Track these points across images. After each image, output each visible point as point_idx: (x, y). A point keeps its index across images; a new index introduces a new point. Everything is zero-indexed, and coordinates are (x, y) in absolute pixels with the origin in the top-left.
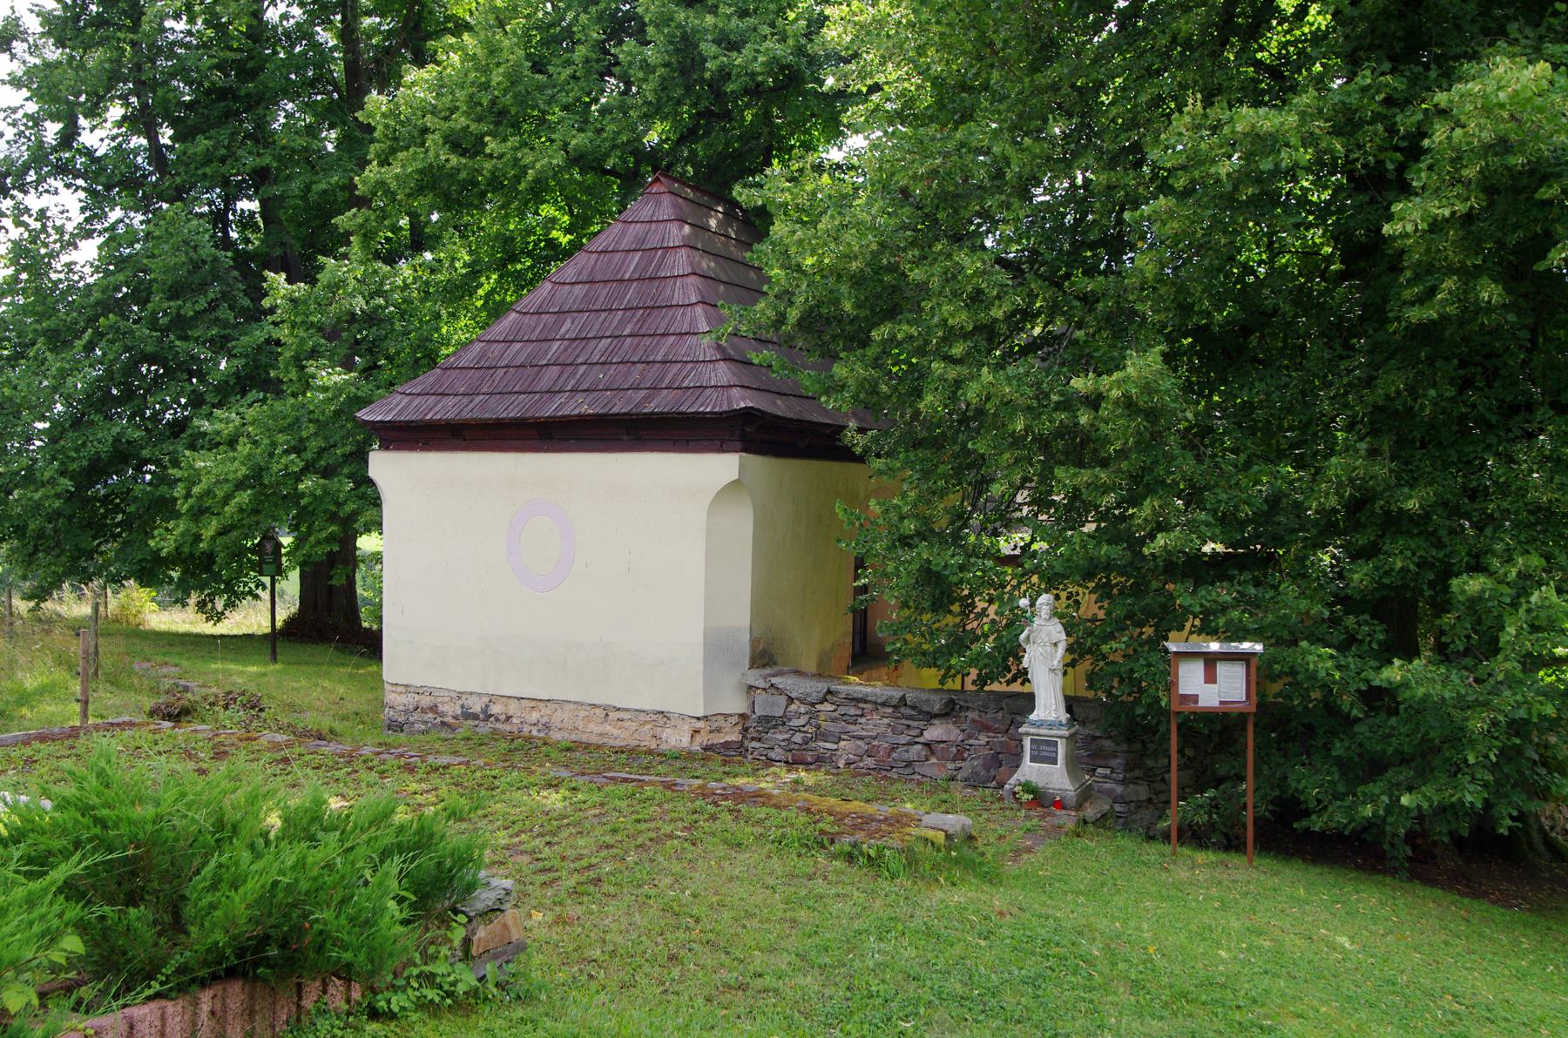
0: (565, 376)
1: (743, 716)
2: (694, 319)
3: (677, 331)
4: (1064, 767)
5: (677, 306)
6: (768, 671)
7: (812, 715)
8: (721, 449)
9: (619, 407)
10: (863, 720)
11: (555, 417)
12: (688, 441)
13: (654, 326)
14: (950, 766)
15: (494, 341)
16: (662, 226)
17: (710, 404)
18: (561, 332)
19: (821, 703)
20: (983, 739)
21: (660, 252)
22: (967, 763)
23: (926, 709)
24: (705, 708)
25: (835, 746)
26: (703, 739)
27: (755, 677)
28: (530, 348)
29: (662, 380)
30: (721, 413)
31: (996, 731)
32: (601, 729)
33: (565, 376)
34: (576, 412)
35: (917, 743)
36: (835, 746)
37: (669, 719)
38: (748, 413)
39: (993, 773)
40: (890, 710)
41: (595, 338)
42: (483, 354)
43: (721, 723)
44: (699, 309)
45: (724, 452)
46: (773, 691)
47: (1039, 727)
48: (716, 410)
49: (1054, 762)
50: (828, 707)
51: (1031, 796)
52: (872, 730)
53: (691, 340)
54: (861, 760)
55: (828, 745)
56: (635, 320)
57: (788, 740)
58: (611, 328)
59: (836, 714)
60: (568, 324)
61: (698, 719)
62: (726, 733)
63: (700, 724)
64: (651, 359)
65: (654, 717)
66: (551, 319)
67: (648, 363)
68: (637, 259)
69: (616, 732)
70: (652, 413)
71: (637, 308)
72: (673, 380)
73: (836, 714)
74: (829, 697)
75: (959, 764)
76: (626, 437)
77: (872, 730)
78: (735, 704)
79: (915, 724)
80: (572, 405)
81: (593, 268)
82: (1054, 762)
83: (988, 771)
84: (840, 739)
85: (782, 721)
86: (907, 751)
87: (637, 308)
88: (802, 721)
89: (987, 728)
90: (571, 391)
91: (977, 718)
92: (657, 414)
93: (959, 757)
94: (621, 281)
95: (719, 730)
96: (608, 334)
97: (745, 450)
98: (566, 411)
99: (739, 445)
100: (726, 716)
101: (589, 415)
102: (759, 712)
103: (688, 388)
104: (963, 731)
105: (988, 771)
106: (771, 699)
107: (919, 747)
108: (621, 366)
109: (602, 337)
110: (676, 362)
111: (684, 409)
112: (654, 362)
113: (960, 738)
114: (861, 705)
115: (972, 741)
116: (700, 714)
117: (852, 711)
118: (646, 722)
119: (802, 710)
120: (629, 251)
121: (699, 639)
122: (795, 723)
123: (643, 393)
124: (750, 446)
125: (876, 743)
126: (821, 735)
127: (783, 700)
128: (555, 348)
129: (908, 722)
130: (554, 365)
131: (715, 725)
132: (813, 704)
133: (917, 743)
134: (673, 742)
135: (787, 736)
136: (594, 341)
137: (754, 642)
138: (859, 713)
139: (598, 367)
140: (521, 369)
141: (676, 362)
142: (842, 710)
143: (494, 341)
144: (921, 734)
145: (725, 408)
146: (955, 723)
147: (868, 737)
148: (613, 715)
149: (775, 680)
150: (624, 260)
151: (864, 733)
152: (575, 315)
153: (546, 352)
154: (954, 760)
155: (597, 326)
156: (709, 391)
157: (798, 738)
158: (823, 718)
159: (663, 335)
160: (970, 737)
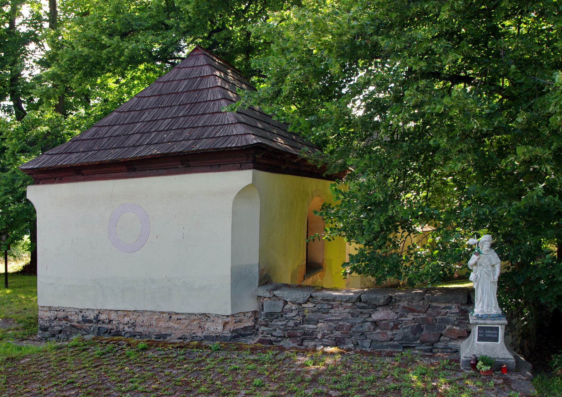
0: (144, 138)
1: (255, 312)
2: (220, 105)
3: (211, 112)
4: (503, 343)
5: (210, 101)
6: (270, 287)
7: (301, 310)
8: (241, 168)
9: (177, 148)
10: (332, 311)
11: (136, 157)
12: (219, 165)
13: (196, 111)
14: (389, 333)
15: (103, 126)
16: (199, 68)
17: (234, 143)
18: (142, 118)
19: (306, 303)
20: (410, 317)
21: (199, 79)
22: (401, 330)
23: (374, 302)
24: (232, 310)
25: (315, 327)
26: (231, 327)
27: (263, 292)
28: (124, 127)
29: (203, 134)
30: (242, 147)
31: (419, 312)
32: (167, 325)
33: (144, 138)
34: (150, 153)
35: (367, 321)
36: (315, 327)
37: (209, 317)
38: (257, 147)
39: (418, 336)
40: (350, 304)
41: (162, 119)
42: (96, 132)
43: (243, 317)
44: (223, 102)
45: (242, 169)
46: (275, 298)
47: (485, 319)
48: (239, 145)
49: (496, 340)
50: (310, 305)
51: (489, 368)
52: (339, 316)
53: (218, 115)
54: (332, 333)
55: (310, 326)
56: (186, 109)
57: (285, 325)
58: (172, 114)
59: (315, 308)
60: (146, 114)
61: (228, 316)
62: (245, 322)
63: (229, 319)
64: (196, 125)
65: (200, 317)
66: (138, 113)
67: (194, 128)
68: (186, 83)
69: (176, 326)
70: (198, 150)
71: (186, 104)
72: (210, 134)
73: (315, 308)
74: (310, 300)
75: (395, 332)
76: (181, 166)
77: (339, 316)
78: (251, 306)
79: (366, 311)
80: (147, 150)
81: (161, 89)
82: (496, 340)
83: (415, 334)
84: (318, 322)
85: (282, 315)
86: (361, 327)
87: (186, 104)
88: (294, 314)
89: (412, 311)
90: (147, 144)
91: (406, 305)
92: (200, 150)
93: (395, 327)
94: (177, 93)
95: (240, 321)
96: (169, 117)
97: (255, 168)
98: (143, 154)
99: (251, 165)
100: (244, 314)
101: (157, 154)
102: (266, 310)
103: (219, 137)
104: (397, 313)
105: (415, 334)
106: (273, 303)
107: (369, 324)
108: (177, 131)
109: (166, 119)
110: (211, 126)
111: (217, 146)
112: (197, 127)
113: (396, 317)
114: (331, 303)
115: (403, 319)
116: (229, 313)
117: (326, 306)
118: (194, 320)
119: (294, 308)
120: (181, 80)
121: (227, 272)
122: (290, 315)
123: (191, 142)
124: (257, 166)
125: (341, 323)
126: (305, 321)
127: (281, 303)
128: (138, 126)
129: (361, 310)
130: (137, 133)
131: (238, 319)
132: (300, 304)
133: (367, 321)
134: (212, 329)
135: (284, 323)
136: (161, 121)
137: (261, 271)
138: (330, 307)
139: (163, 132)
140: (117, 138)
141: (211, 126)
142: (319, 306)
143: (103, 126)
144: (370, 316)
145: (244, 144)
146: (391, 309)
147: (336, 320)
148: (174, 317)
149: (276, 293)
150: (179, 84)
151: (334, 318)
152: (150, 110)
153: (133, 128)
154: (392, 329)
155: (163, 114)
156: (232, 138)
157: (291, 323)
158: (307, 311)
159: (203, 114)
160: (402, 316)
